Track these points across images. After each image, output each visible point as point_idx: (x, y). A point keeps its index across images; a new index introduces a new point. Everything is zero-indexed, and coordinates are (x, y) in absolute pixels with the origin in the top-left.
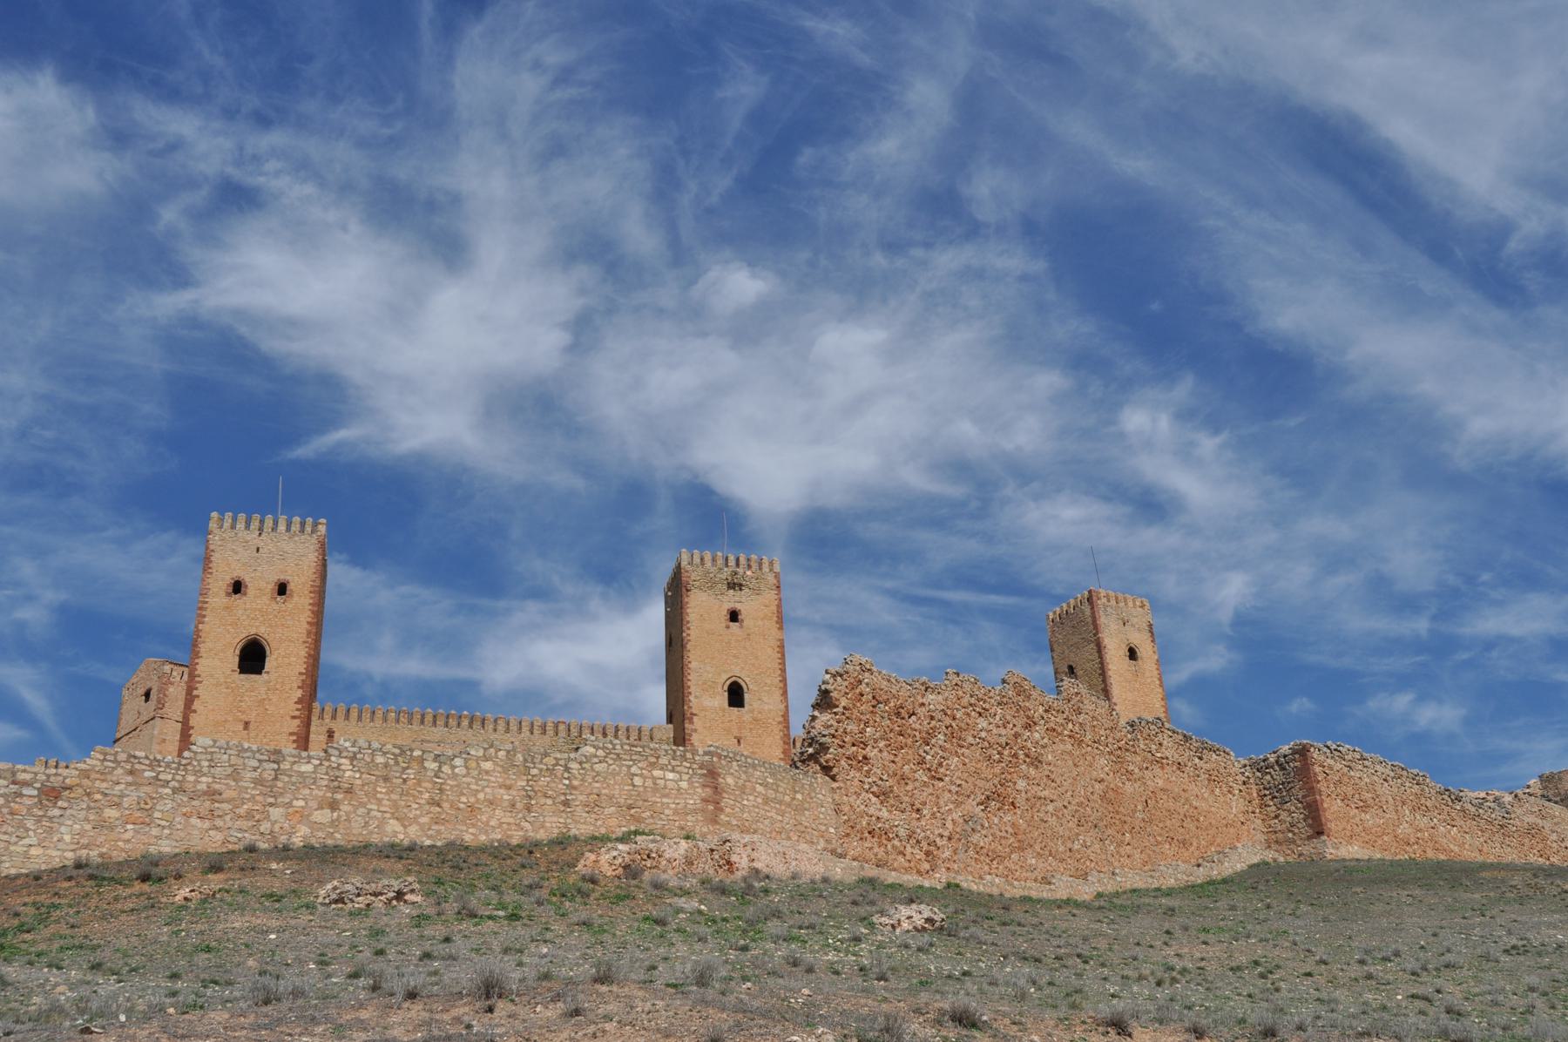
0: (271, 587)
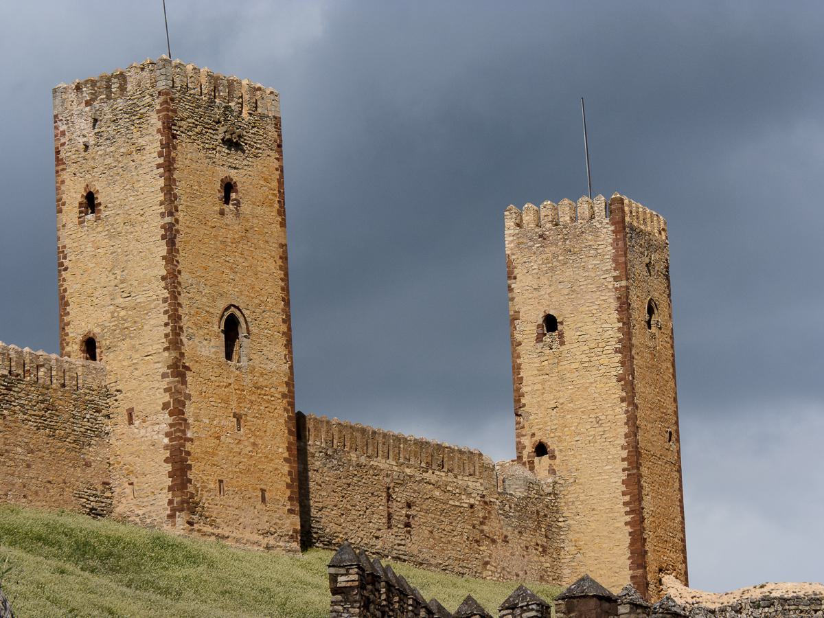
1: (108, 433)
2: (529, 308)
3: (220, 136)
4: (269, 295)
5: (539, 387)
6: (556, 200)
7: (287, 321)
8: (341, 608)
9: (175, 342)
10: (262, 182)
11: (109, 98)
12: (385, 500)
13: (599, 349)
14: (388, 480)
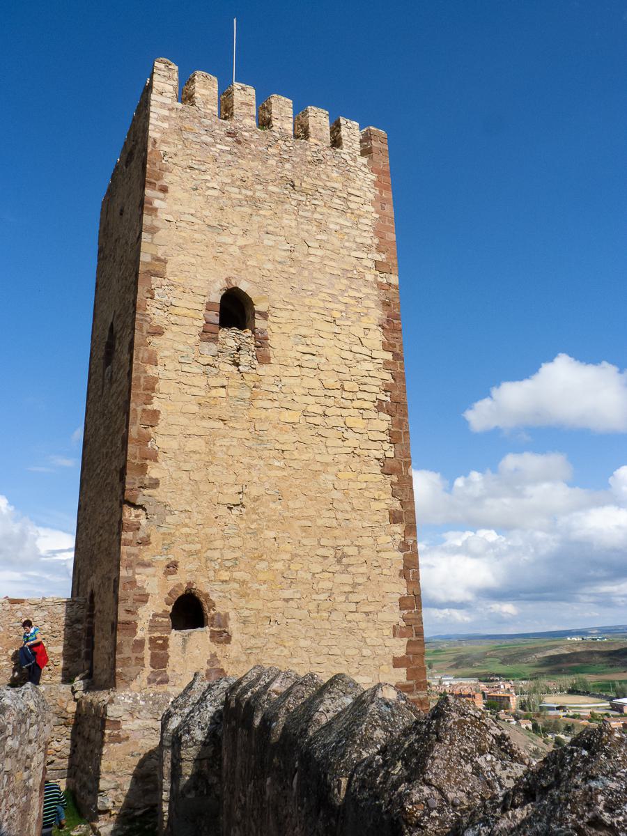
2: (193, 261)
5: (192, 444)
13: (345, 395)
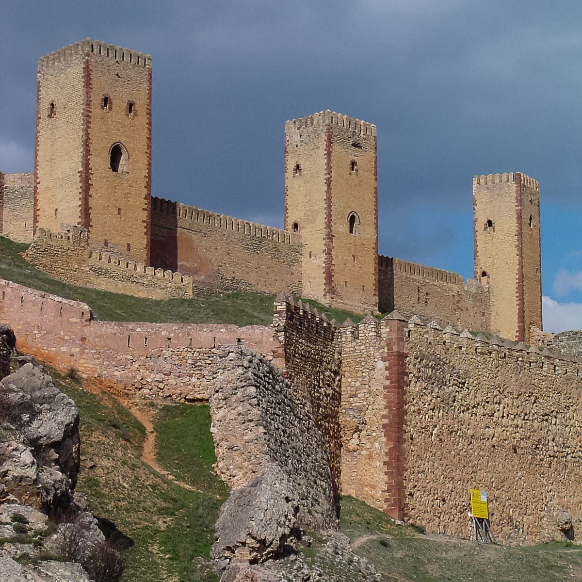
0: (125, 105)
1: (301, 261)
3: (351, 143)
4: (369, 208)
6: (494, 173)
7: (376, 218)
8: (278, 320)
9: (329, 225)
10: (368, 162)
11: (306, 127)
12: (417, 292)
14: (418, 284)
